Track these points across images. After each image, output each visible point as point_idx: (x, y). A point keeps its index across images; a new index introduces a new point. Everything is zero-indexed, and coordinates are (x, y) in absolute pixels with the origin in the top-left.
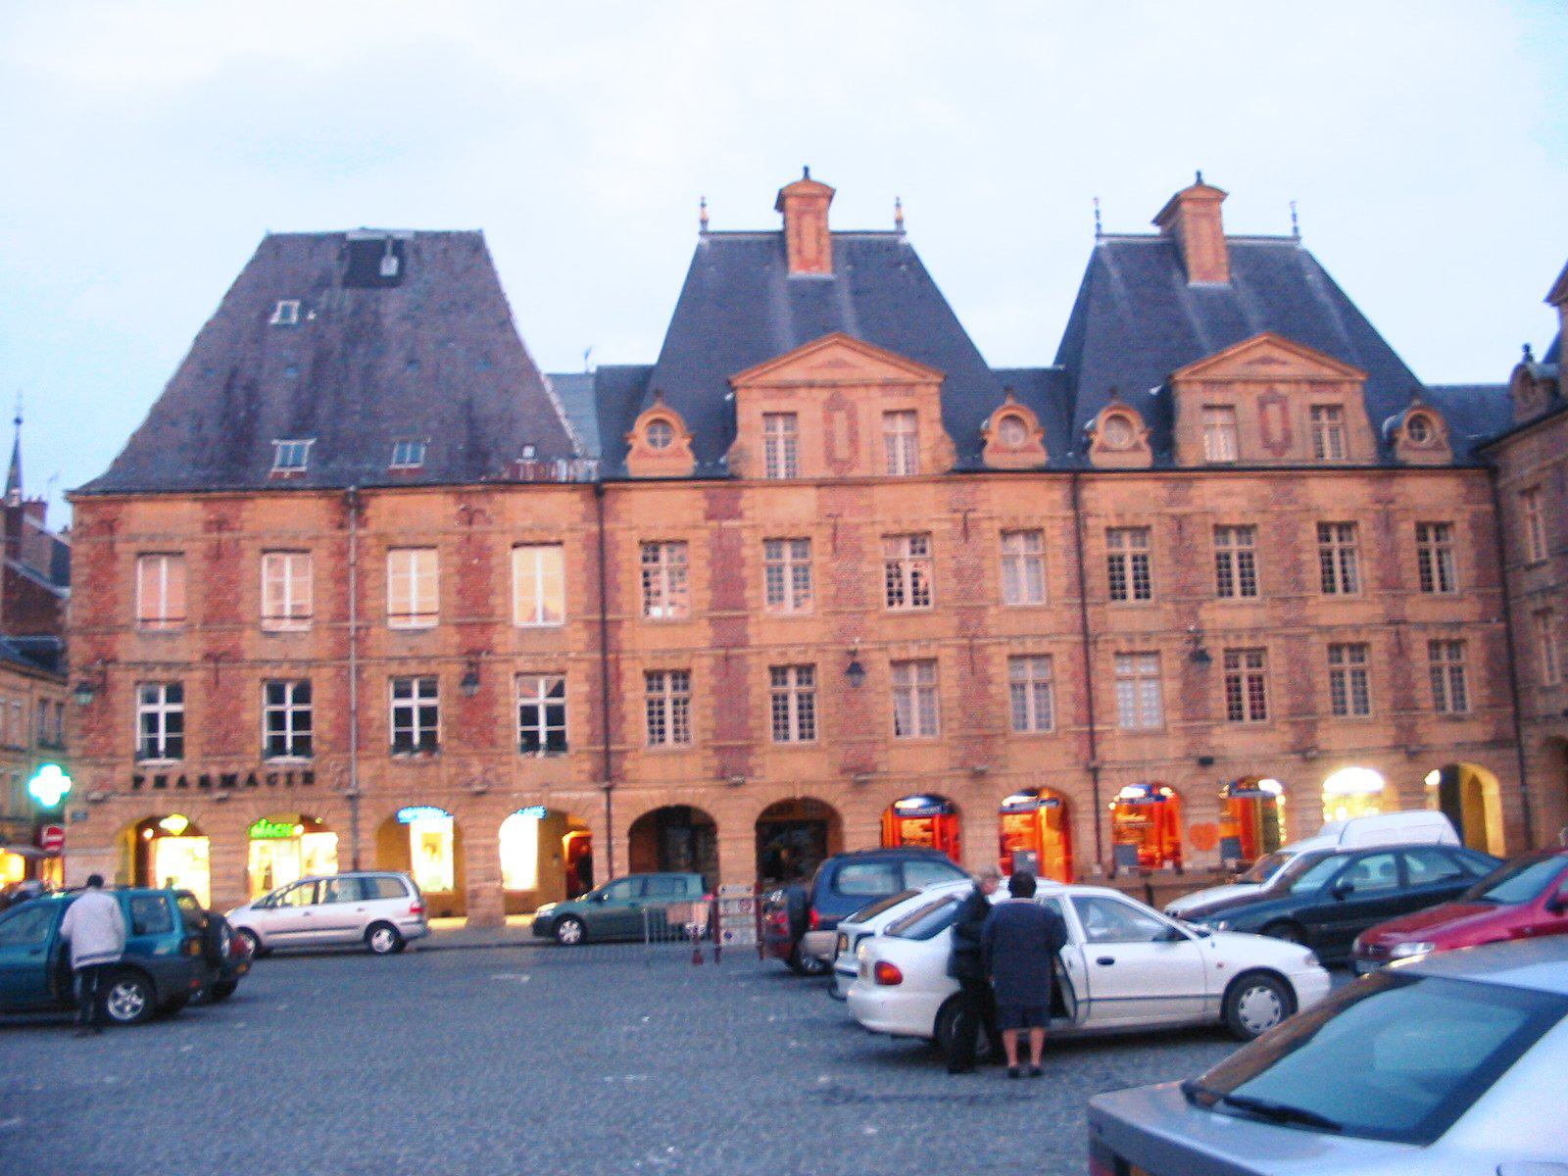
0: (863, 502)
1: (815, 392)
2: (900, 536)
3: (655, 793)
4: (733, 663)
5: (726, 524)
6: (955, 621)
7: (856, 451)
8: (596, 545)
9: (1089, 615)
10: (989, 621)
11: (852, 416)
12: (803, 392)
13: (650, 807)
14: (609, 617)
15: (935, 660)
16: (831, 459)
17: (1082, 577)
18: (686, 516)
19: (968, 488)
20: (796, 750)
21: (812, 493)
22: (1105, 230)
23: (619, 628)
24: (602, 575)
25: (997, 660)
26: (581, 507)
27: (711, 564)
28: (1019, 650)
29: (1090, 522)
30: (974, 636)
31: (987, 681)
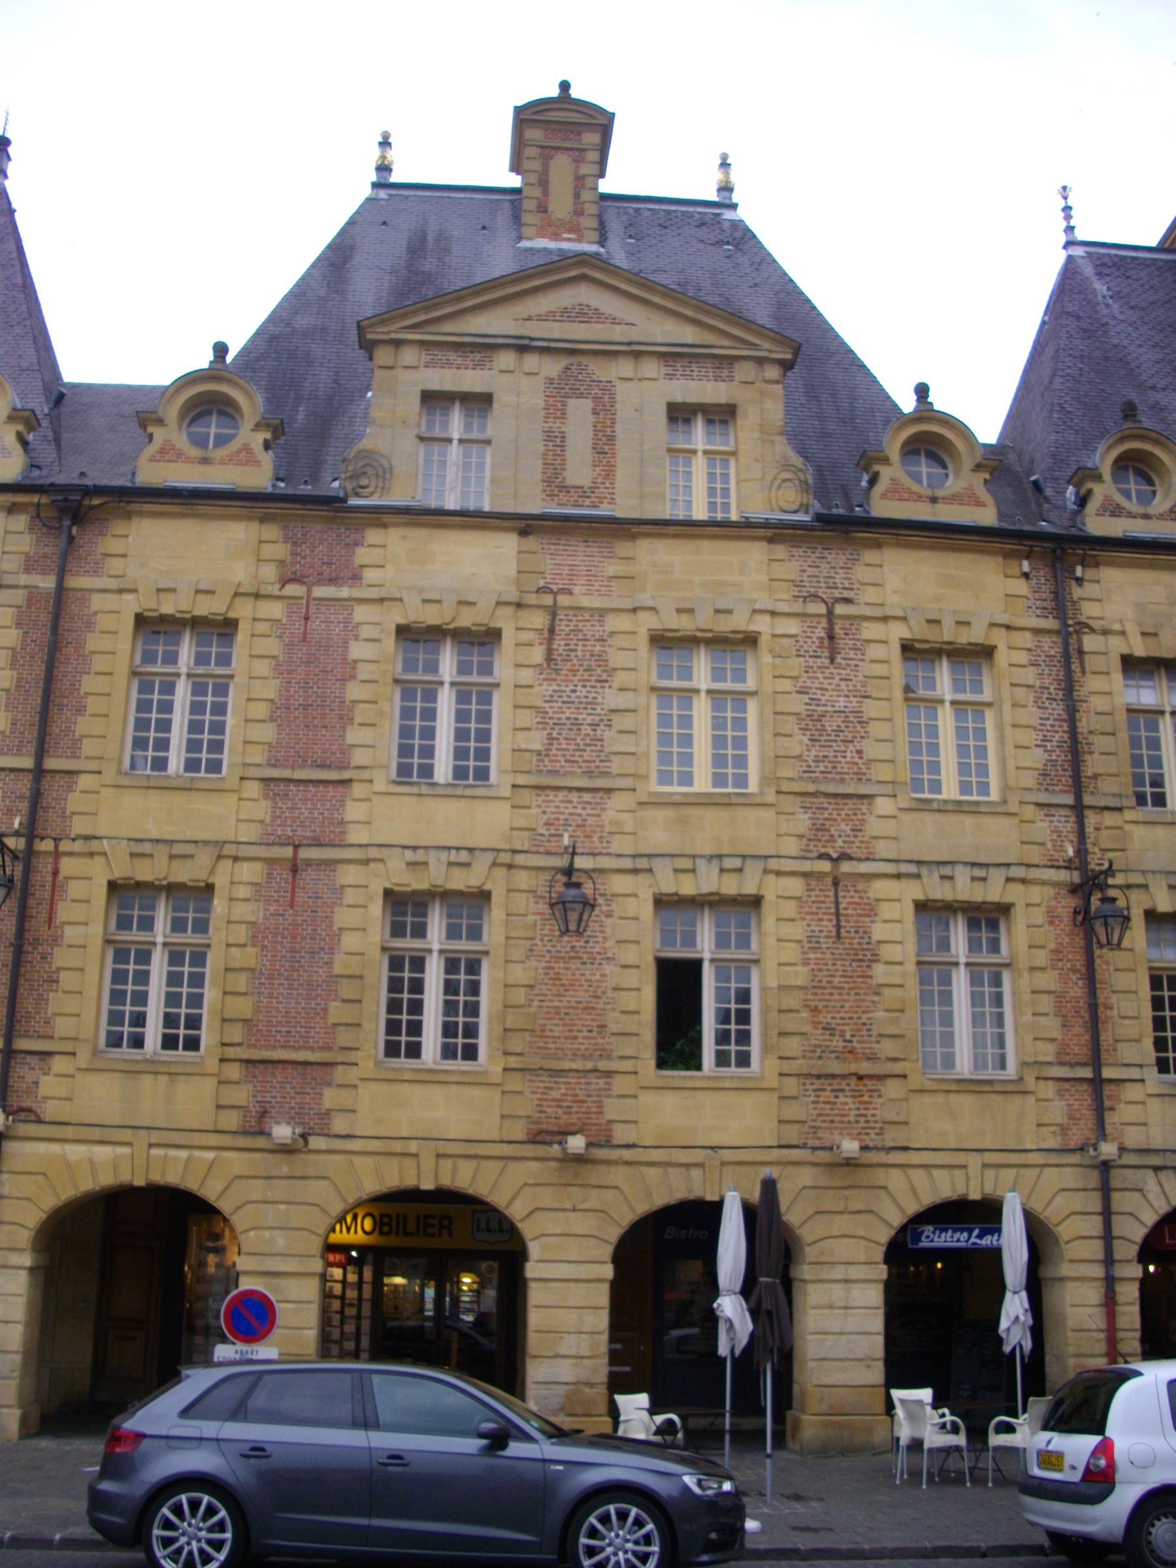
0: (612, 569)
1: (531, 361)
2: (691, 641)
3: (103, 1153)
4: (308, 877)
5: (320, 592)
6: (803, 822)
7: (609, 473)
8: (45, 617)
9: (1089, 830)
10: (874, 827)
11: (604, 408)
12: (506, 359)
13: (88, 1184)
14: (50, 763)
15: (756, 902)
16: (554, 483)
17: (1075, 750)
18: (241, 573)
19: (837, 557)
20: (431, 1078)
21: (507, 544)
22: (1080, 235)
23: (70, 789)
24: (49, 679)
25: (887, 911)
26: (24, 543)
27: (281, 668)
28: (939, 891)
29: (1090, 642)
30: (845, 857)
31: (868, 955)
